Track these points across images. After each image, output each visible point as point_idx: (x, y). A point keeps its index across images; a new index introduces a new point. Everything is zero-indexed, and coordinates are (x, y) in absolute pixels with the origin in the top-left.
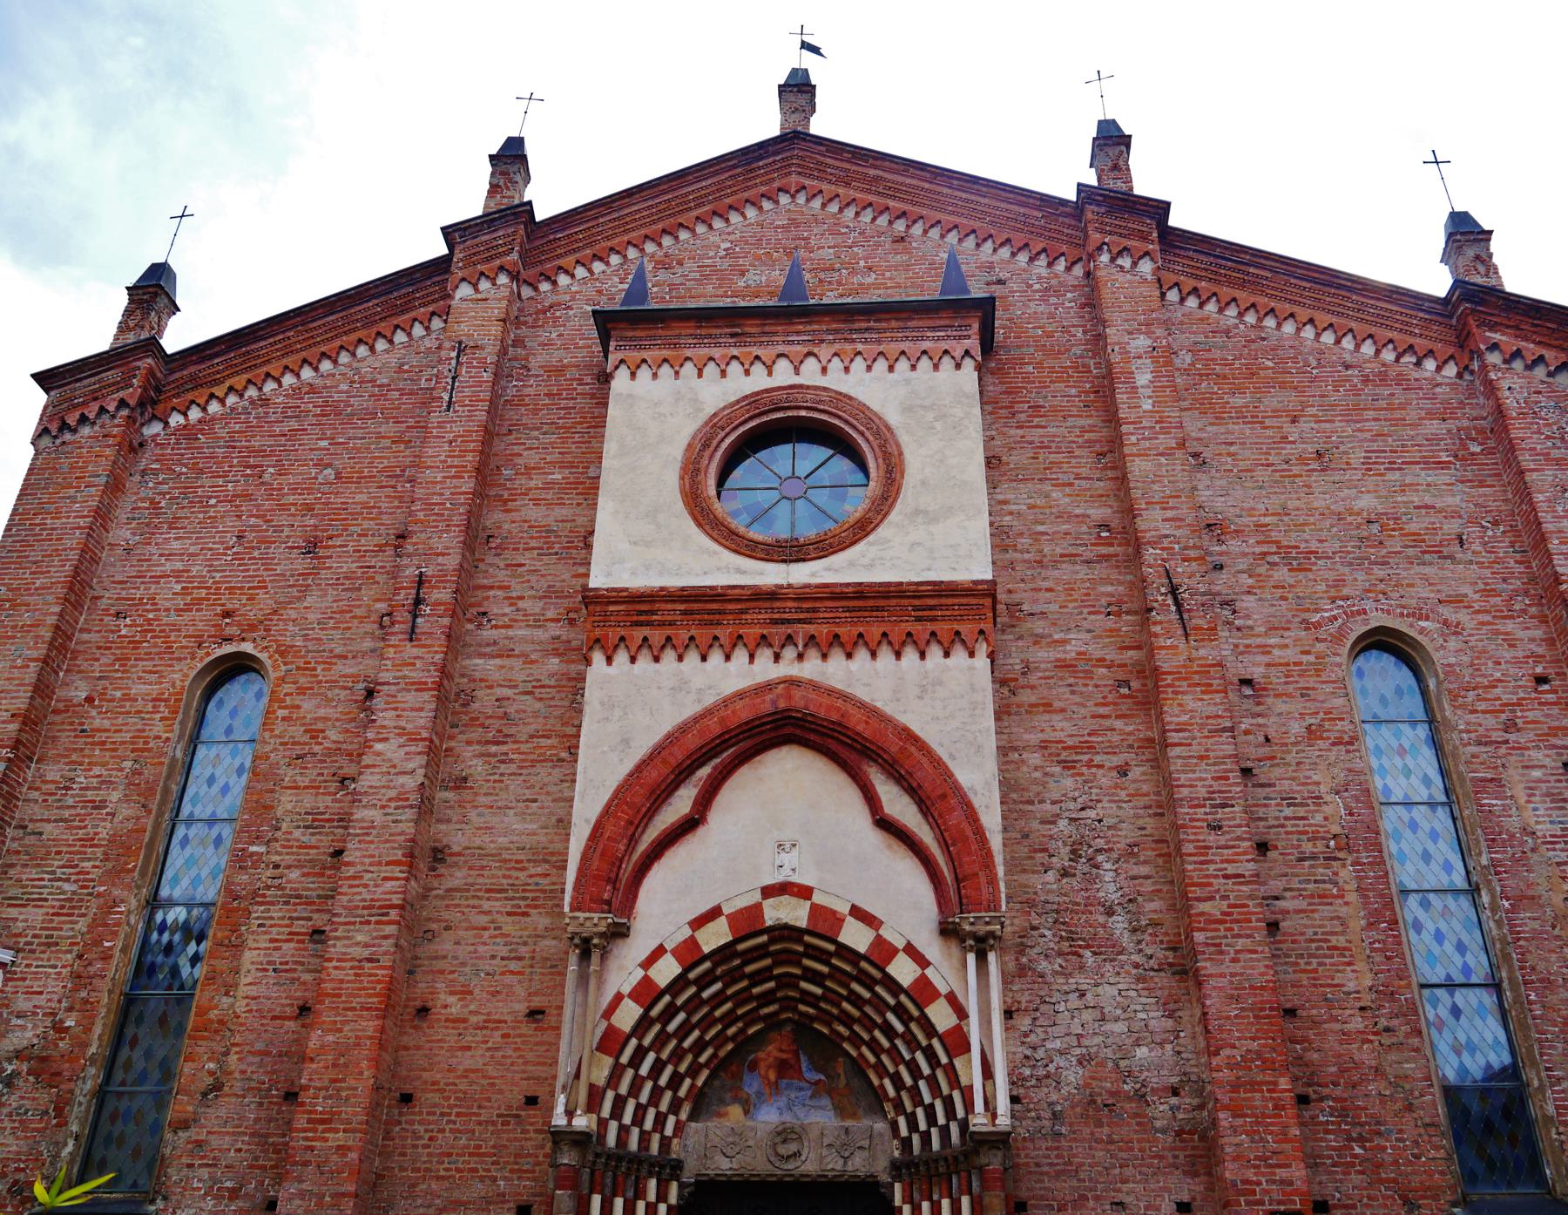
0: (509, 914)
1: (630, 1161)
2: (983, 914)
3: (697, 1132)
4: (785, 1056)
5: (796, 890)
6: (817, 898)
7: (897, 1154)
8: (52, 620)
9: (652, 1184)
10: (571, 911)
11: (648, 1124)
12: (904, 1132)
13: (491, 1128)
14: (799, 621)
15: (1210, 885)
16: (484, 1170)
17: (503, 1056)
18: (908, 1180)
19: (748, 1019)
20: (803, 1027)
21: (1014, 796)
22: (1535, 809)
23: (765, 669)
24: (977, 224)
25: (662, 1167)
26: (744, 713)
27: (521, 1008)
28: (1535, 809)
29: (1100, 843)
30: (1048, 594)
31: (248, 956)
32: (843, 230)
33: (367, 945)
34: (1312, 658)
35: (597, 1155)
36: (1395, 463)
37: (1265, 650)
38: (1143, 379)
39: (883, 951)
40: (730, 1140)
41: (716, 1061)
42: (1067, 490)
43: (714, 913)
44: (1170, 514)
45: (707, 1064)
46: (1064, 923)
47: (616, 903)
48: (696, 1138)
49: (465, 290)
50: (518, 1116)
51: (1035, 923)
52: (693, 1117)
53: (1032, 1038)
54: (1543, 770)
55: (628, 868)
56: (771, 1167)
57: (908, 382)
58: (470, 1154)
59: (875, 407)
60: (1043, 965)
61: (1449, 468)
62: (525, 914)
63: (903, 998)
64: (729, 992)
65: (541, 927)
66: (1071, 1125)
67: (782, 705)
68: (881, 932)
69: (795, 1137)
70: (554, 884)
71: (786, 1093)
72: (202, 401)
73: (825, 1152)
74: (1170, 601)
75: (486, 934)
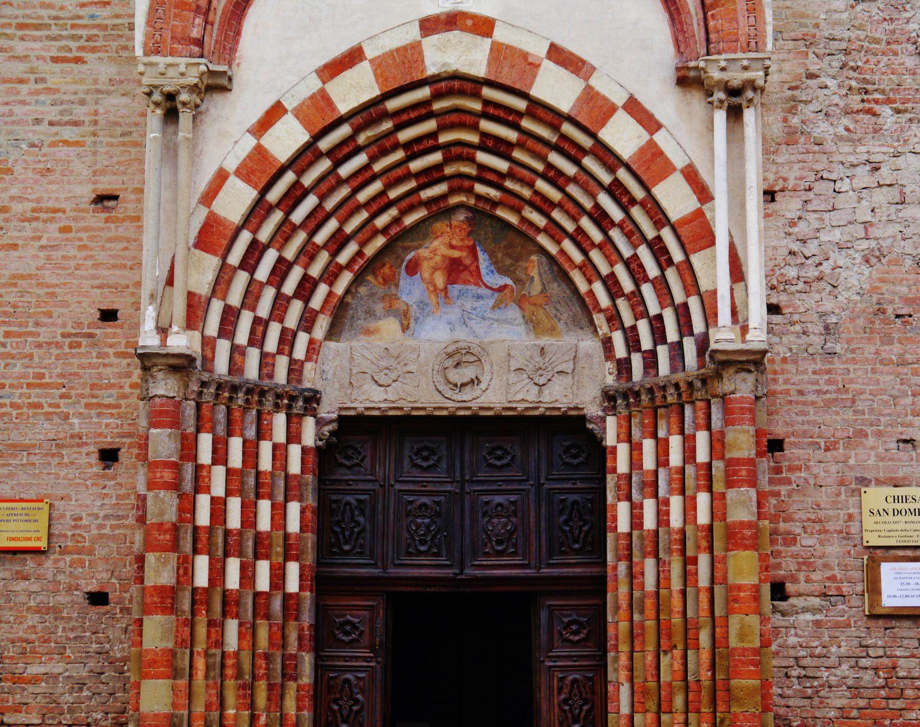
0: (55, 60)
1: (249, 391)
2: (739, 55)
3: (337, 354)
4: (456, 254)
5: (469, 22)
6: (501, 34)
7: (610, 380)
9: (280, 420)
10: (146, 54)
11: (271, 344)
12: (620, 351)
13: (55, 351)
16: (50, 405)
17: (64, 257)
18: (625, 412)
19: (404, 204)
25: (292, 399)
27: (86, 192)
35: (204, 384)
40: (384, 363)
41: (361, 262)
43: (353, 57)
45: (349, 266)
46: (854, 69)
47: (210, 43)
48: (337, 362)
50: (91, 336)
51: (813, 69)
52: (333, 333)
53: (802, 229)
56: (439, 398)
58: (29, 385)
60: (822, 129)
62: (78, 60)
63: (622, 174)
64: (378, 167)
65: (103, 79)
66: (849, 341)
68: (593, 82)
69: (472, 359)
70: (117, 16)
71: (459, 302)
73: (513, 378)
75: (24, 88)
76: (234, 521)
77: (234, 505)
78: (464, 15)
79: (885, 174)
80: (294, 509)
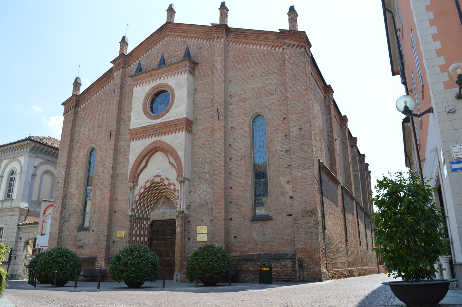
6: (162, 177)
8: (68, 145)
14: (158, 130)
15: (217, 168)
20: (166, 197)
21: (194, 155)
22: (278, 146)
23: (153, 139)
24: (197, 36)
26: (150, 148)
28: (278, 146)
29: (206, 161)
30: (202, 115)
31: (97, 193)
32: (175, 43)
33: (107, 191)
34: (244, 121)
36: (266, 74)
37: (236, 120)
38: (219, 67)
39: (170, 184)
42: (207, 93)
44: (219, 96)
45: (153, 203)
49: (115, 73)
54: (281, 138)
55: (136, 175)
57: (177, 79)
59: (171, 85)
60: (196, 184)
61: (276, 73)
67: (155, 145)
72: (84, 102)
74: (217, 115)
76: (138, 233)
77: (138, 231)
78: (158, 175)
79: (202, 189)
80: (146, 231)
